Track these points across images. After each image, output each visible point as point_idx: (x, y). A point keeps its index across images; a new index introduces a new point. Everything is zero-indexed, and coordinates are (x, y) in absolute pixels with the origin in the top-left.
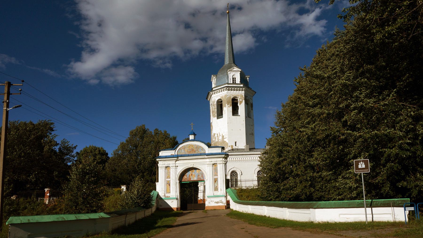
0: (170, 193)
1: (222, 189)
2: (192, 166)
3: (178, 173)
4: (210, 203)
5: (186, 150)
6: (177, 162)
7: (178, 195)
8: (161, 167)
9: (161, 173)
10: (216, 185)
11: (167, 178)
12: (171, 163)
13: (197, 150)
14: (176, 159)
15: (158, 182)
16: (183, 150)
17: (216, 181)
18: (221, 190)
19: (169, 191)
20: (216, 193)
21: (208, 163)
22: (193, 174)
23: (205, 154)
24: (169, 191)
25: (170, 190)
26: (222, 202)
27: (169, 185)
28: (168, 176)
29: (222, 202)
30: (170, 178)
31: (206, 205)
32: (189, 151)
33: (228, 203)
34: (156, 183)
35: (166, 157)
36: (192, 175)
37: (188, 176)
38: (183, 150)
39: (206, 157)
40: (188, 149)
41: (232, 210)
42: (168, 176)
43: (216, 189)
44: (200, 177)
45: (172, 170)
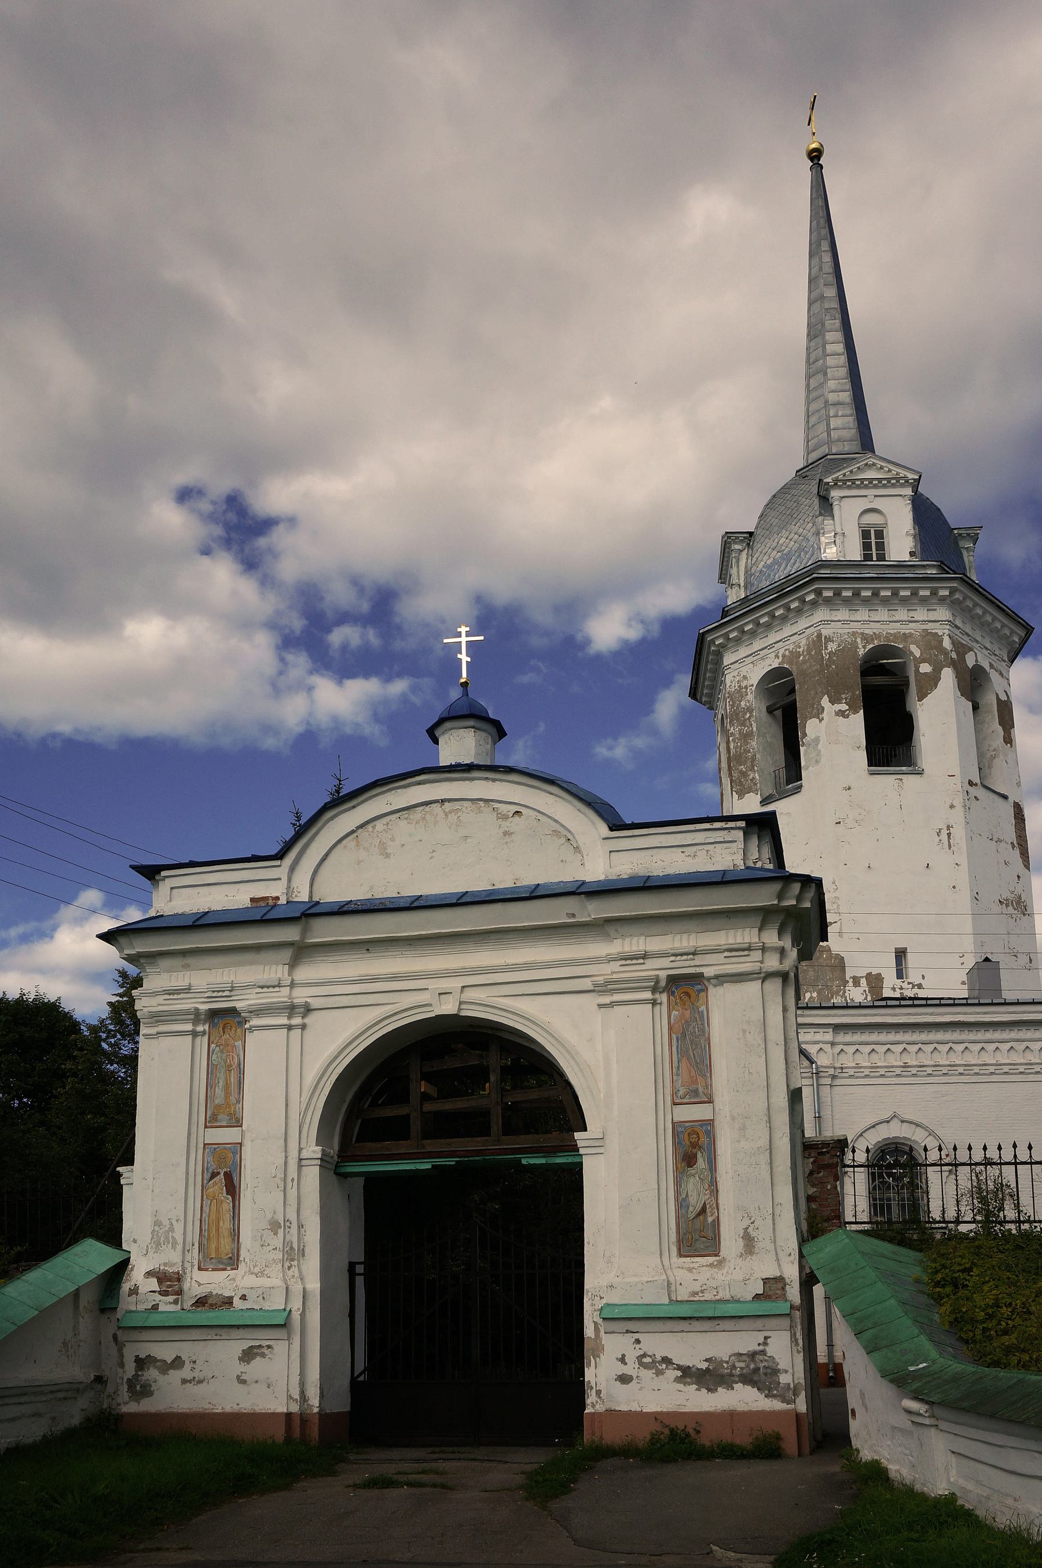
0: (233, 1261)
2: (448, 1007)
4: (624, 1381)
6: (306, 972)
7: (314, 1285)
8: (158, 1018)
10: (695, 1192)
11: (212, 1122)
12: (248, 980)
17: (693, 1148)
18: (749, 1242)
20: (696, 1278)
26: (758, 1373)
27: (232, 1188)
28: (222, 1106)
29: (758, 1373)
31: (593, 1405)
33: (826, 1378)
41: (877, 1473)
43: (697, 1235)
45: (263, 1051)
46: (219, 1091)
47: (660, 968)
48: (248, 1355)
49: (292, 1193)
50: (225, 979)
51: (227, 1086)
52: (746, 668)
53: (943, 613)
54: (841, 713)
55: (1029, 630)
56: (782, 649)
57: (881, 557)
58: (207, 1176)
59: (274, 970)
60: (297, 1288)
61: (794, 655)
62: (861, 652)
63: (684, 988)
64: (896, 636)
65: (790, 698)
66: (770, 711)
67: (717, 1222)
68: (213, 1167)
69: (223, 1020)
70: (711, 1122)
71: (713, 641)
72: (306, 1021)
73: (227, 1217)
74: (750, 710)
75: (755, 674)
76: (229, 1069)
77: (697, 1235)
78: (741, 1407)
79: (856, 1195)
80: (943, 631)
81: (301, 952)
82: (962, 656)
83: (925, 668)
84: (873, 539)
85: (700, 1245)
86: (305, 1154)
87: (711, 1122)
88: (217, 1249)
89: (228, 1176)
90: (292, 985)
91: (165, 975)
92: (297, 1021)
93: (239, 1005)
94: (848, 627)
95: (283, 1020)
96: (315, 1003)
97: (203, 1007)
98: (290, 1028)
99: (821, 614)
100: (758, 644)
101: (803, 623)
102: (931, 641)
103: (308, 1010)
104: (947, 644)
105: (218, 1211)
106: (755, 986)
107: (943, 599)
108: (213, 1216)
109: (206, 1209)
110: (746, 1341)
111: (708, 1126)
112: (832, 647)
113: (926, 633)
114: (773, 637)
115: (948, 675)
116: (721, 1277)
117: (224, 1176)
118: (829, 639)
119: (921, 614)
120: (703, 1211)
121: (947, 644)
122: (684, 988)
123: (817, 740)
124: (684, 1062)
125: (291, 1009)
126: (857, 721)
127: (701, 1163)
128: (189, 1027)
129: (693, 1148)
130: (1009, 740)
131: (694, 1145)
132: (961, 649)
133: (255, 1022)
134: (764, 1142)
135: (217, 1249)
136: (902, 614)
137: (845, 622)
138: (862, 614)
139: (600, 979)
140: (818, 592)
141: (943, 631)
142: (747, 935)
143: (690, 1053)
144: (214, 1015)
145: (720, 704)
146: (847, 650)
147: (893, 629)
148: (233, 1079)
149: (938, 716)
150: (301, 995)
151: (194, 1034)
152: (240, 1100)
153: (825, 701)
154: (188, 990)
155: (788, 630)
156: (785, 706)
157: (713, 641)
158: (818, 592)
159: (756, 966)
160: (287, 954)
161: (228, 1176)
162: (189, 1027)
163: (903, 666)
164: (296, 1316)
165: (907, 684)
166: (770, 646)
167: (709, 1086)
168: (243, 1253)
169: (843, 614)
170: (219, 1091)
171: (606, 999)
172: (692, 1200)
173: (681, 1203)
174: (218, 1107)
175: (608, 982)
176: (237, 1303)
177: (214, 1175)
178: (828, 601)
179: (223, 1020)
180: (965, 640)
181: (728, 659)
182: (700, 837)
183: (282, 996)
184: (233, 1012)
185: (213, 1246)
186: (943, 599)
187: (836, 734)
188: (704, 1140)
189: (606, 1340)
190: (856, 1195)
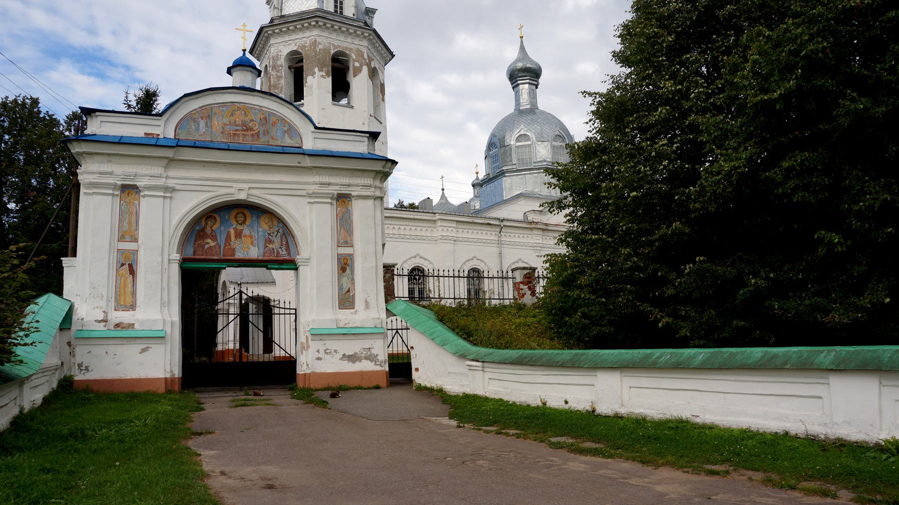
0: (133, 307)
1: (372, 304)
2: (242, 196)
5: (217, 123)
6: (172, 173)
9: (95, 216)
11: (122, 239)
12: (144, 173)
13: (266, 132)
14: (169, 153)
15: (74, 255)
16: (202, 124)
17: (345, 265)
19: (129, 300)
21: (313, 188)
22: (246, 231)
23: (301, 152)
24: (129, 300)
25: (134, 294)
27: (132, 271)
30: (136, 240)
32: (230, 129)
34: (66, 261)
35: (120, 142)
36: (239, 235)
37: (222, 239)
38: (202, 124)
39: (308, 162)
40: (226, 120)
42: (127, 231)
43: (346, 300)
44: (276, 245)
46: (126, 224)
48: (144, 350)
49: (166, 276)
50: (131, 170)
51: (130, 223)
52: (281, 48)
53: (365, 43)
54: (323, 76)
55: (393, 56)
56: (298, 42)
57: (341, 13)
58: (119, 265)
59: (158, 170)
60: (168, 319)
61: (303, 47)
62: (332, 52)
64: (346, 48)
65: (300, 65)
66: (290, 68)
67: (354, 296)
68: (122, 261)
69: (129, 190)
70: (352, 255)
71: (267, 32)
72: (173, 195)
73: (130, 285)
74: (281, 66)
75: (285, 51)
76: (131, 214)
77: (346, 300)
78: (365, 369)
79: (402, 287)
80: (365, 50)
81: (171, 162)
82: (370, 62)
83: (357, 64)
85: (347, 304)
86: (171, 257)
87: (352, 255)
88: (124, 301)
89: (130, 266)
90: (167, 177)
91: (97, 165)
92: (168, 195)
93: (138, 184)
94: (328, 41)
95: (162, 194)
96: (177, 187)
97: (119, 183)
98: (165, 197)
99: (316, 32)
100: (286, 38)
101: (307, 34)
102: (360, 54)
103: (173, 190)
104: (365, 56)
105: (125, 282)
106: (371, 202)
107: (365, 37)
108: (122, 284)
109: (119, 281)
110: (366, 343)
112: (321, 47)
113: (358, 50)
114: (294, 37)
115: (365, 69)
116: (357, 317)
117: (129, 266)
118: (319, 43)
119: (357, 41)
120: (349, 291)
121: (365, 56)
123: (311, 86)
124: (342, 230)
125: (166, 189)
126: (329, 81)
127: (348, 271)
128: (111, 192)
129: (345, 265)
130: (383, 100)
131: (345, 264)
132: (371, 59)
133: (147, 193)
134: (374, 264)
135: (124, 301)
136: (349, 40)
137: (327, 38)
138: (334, 36)
139: (311, 192)
140: (317, 22)
141: (365, 50)
142: (369, 181)
143: (344, 225)
145: (265, 60)
146: (327, 50)
147: (345, 45)
148: (133, 219)
149: (359, 83)
150: (171, 183)
151: (113, 195)
152: (137, 229)
153: (316, 70)
154: (111, 173)
155: (300, 35)
156: (297, 69)
157: (267, 32)
158: (317, 22)
159: (372, 194)
160: (165, 162)
161: (130, 266)
162: (111, 192)
163: (347, 61)
164: (169, 331)
165: (348, 68)
166: (293, 40)
167: (352, 240)
168: (138, 303)
169: (326, 34)
170: (126, 224)
171: (312, 201)
172: (344, 286)
173: (340, 288)
174: (126, 232)
175: (314, 193)
176: (136, 326)
177: (123, 265)
178: (320, 27)
179: (129, 190)
180: (371, 56)
181: (272, 41)
182: (351, 138)
183: (161, 182)
184: (135, 187)
185: (122, 299)
186: (365, 37)
187: (318, 85)
188: (349, 262)
189: (310, 343)
190: (402, 287)
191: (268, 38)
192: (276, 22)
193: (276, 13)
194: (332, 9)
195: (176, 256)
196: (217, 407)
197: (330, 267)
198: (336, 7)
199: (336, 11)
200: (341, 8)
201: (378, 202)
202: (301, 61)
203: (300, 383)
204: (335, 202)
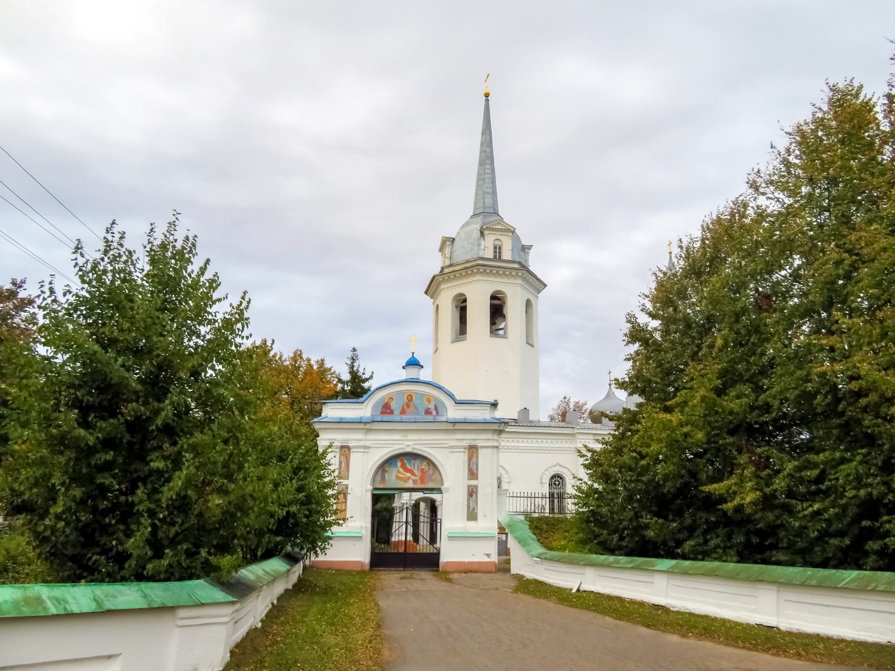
2: (409, 450)
3: (369, 467)
4: (450, 553)
12: (352, 438)
17: (472, 492)
21: (452, 443)
31: (444, 558)
35: (341, 422)
43: (472, 516)
47: (466, 443)
57: (500, 257)
59: (360, 436)
63: (473, 450)
65: (464, 304)
66: (457, 307)
77: (472, 516)
81: (369, 431)
84: (498, 249)
103: (369, 447)
106: (490, 450)
111: (476, 487)
122: (473, 450)
125: (365, 447)
129: (472, 492)
142: (489, 436)
144: (342, 447)
150: (368, 443)
160: (364, 431)
173: (469, 507)
181: (442, 287)
184: (348, 448)
191: (439, 284)
192: (446, 271)
193: (447, 263)
194: (492, 257)
195: (370, 487)
196: (391, 578)
197: (463, 494)
198: (495, 252)
199: (495, 257)
200: (500, 253)
201: (495, 450)
202: (465, 301)
203: (441, 569)
204: (467, 451)
